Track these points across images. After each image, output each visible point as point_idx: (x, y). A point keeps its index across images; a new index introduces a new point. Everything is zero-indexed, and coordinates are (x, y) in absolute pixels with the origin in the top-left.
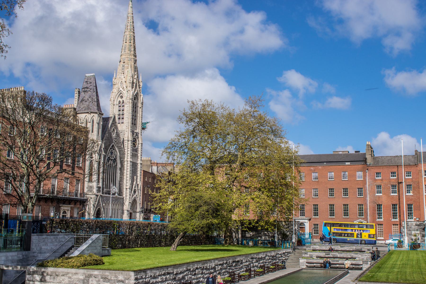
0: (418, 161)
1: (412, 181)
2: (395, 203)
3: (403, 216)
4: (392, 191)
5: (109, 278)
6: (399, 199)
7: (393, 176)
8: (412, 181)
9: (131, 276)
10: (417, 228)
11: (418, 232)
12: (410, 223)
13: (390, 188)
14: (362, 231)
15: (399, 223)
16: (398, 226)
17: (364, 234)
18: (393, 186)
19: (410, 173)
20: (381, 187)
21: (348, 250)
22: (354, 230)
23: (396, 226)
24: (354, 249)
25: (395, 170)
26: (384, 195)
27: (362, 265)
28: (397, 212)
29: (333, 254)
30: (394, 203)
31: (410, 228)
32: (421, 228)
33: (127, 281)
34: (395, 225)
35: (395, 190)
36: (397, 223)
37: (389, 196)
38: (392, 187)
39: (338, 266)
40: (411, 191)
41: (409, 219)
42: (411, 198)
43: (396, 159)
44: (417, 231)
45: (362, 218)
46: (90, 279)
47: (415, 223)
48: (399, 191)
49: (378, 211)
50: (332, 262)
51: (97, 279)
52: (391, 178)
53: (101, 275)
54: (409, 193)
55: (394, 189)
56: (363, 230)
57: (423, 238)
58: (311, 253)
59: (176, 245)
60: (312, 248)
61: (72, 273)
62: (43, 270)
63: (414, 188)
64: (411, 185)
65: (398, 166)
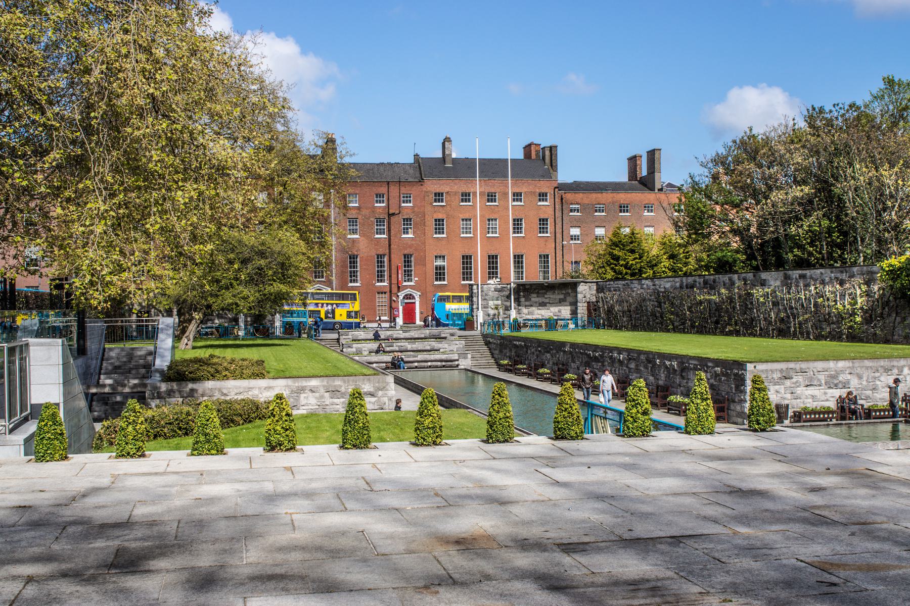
0: (423, 176)
1: (413, 212)
2: (381, 253)
3: (396, 276)
4: (377, 229)
5: (343, 389)
6: (390, 245)
8: (413, 212)
9: (388, 384)
10: (497, 296)
11: (499, 302)
12: (485, 286)
13: (373, 224)
14: (335, 306)
15: (388, 290)
16: (387, 295)
17: (338, 311)
18: (380, 221)
19: (410, 197)
20: (356, 222)
21: (416, 336)
22: (320, 305)
23: (384, 295)
24: (427, 335)
25: (383, 190)
26: (363, 238)
27: (458, 360)
28: (385, 269)
29: (399, 344)
30: (381, 252)
31: (486, 295)
32: (503, 296)
33: (380, 393)
34: (382, 293)
35: (382, 227)
38: (377, 222)
39: (416, 364)
40: (410, 230)
41: (405, 281)
42: (410, 243)
43: (382, 169)
45: (321, 281)
46: (302, 396)
47: (494, 286)
48: (389, 230)
49: (351, 268)
51: (317, 395)
52: (376, 205)
53: (324, 386)
54: (407, 233)
55: (380, 225)
56: (336, 304)
57: (506, 312)
58: (359, 346)
59: (191, 337)
60: (350, 337)
61: (260, 388)
62: (191, 385)
63: (416, 224)
64: (411, 219)
65: (388, 183)
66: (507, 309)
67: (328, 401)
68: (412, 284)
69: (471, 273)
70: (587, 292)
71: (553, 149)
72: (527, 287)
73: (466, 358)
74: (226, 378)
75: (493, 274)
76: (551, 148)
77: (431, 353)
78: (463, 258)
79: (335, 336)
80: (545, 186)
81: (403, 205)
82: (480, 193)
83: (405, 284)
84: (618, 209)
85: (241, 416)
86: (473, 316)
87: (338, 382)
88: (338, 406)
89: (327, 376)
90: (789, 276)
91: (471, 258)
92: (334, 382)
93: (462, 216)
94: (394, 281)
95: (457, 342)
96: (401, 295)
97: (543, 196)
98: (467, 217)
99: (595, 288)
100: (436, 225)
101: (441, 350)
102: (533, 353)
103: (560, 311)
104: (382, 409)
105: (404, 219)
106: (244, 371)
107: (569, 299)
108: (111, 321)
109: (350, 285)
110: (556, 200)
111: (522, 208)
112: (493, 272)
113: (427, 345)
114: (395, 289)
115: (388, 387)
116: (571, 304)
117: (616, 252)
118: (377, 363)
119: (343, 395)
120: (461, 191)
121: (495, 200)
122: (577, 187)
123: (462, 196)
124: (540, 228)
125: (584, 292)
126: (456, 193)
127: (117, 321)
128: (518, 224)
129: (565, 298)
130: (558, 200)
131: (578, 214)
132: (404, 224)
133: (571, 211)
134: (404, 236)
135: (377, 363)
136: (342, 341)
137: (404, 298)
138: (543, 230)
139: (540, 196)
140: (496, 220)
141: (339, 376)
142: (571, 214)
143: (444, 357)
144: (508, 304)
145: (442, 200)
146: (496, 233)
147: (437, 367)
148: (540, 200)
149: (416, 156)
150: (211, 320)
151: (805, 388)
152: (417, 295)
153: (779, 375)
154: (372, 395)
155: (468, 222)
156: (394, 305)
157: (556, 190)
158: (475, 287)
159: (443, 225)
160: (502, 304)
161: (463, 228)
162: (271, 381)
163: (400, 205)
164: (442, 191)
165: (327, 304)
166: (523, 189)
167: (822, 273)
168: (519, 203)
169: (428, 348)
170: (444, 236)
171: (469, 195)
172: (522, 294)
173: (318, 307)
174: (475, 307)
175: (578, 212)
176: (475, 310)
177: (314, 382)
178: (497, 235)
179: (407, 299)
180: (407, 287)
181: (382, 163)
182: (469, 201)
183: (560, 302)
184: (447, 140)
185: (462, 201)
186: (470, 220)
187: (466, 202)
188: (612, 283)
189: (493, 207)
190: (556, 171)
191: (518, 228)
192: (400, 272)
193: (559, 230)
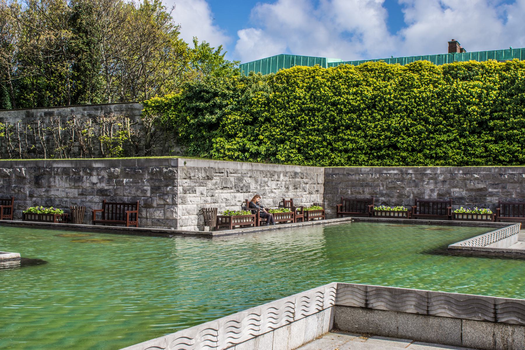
90: (32, 115)
151: (221, 191)
153: (204, 175)
167: (72, 111)
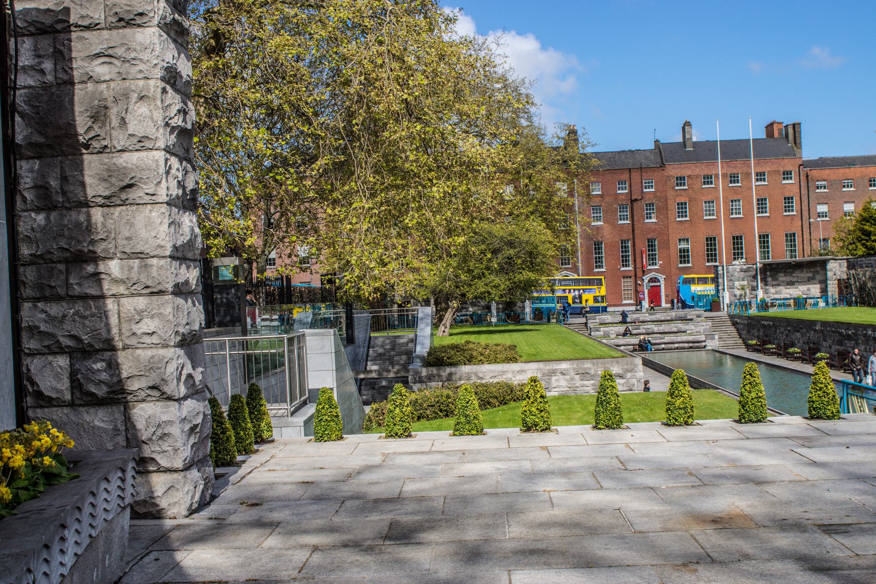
2: (625, 238)
4: (620, 216)
5: (592, 372)
6: (633, 231)
7: (622, 188)
9: (636, 365)
10: (743, 276)
11: (745, 283)
12: (731, 267)
13: (616, 211)
14: (581, 291)
15: (633, 274)
16: (632, 279)
17: (585, 296)
18: (622, 207)
21: (663, 318)
22: (567, 291)
23: (629, 280)
24: (674, 317)
25: (625, 176)
27: (705, 341)
28: (630, 254)
29: (646, 327)
30: (625, 237)
31: (732, 276)
32: (750, 276)
33: (629, 375)
34: (627, 277)
35: (625, 214)
36: (630, 275)
37: (615, 226)
38: (620, 208)
39: (663, 346)
40: (652, 215)
41: (650, 265)
43: (623, 156)
44: (743, 280)
45: (568, 268)
46: (554, 378)
47: (739, 267)
50: (653, 341)
51: (568, 377)
52: (619, 192)
53: (574, 369)
54: (650, 218)
55: (623, 211)
56: (583, 289)
57: (753, 292)
58: (606, 329)
59: (448, 325)
61: (513, 372)
62: (448, 370)
63: (658, 209)
64: (653, 204)
65: (630, 170)
66: (754, 289)
67: (578, 383)
68: (657, 267)
69: (715, 255)
70: (837, 269)
71: (796, 126)
72: (774, 266)
73: (713, 339)
74: (481, 362)
75: (738, 255)
76: (794, 125)
77: (678, 334)
78: (707, 241)
79: (583, 320)
80: (789, 164)
81: (645, 190)
82: (722, 175)
83: (649, 267)
84: (867, 183)
85: (497, 398)
86: (718, 297)
87: (587, 365)
88: (588, 388)
89: (576, 359)
91: (715, 240)
92: (583, 364)
93: (704, 199)
94: (639, 265)
95: (704, 324)
96: (646, 278)
97: (787, 174)
98: (709, 199)
99: (846, 265)
100: (678, 208)
101: (688, 332)
102: (782, 333)
103: (809, 290)
104: (631, 390)
105: (646, 204)
106: (498, 356)
107: (819, 277)
108: (376, 312)
109: (596, 270)
110: (801, 178)
111: (767, 187)
112: (738, 253)
113: (673, 327)
114: (639, 274)
115: (636, 369)
116: (820, 282)
117: (866, 227)
118: (624, 345)
119: (593, 377)
120: (703, 174)
121: (738, 180)
122: (822, 163)
123: (704, 178)
124: (785, 207)
125: (834, 270)
126: (697, 176)
127: (380, 312)
128: (762, 204)
129: (814, 276)
130: (803, 178)
131: (825, 190)
132: (647, 210)
133: (818, 188)
134: (647, 221)
135: (624, 345)
136: (590, 325)
137: (649, 281)
138: (788, 208)
139: (784, 174)
140: (739, 201)
141: (588, 359)
142: (817, 191)
143: (691, 338)
144: (755, 284)
145: (684, 183)
146: (739, 213)
147: (684, 348)
148: (784, 179)
149: (656, 142)
150: (465, 308)
152: (662, 278)
154: (621, 377)
155: (711, 204)
156: (639, 289)
157: (801, 167)
158: (720, 268)
159: (686, 208)
160: (748, 284)
161: (706, 210)
162: (523, 364)
163: (642, 190)
164: (683, 175)
165: (574, 290)
166: (766, 168)
168: (762, 183)
169: (675, 330)
170: (688, 219)
171: (711, 178)
172: (768, 273)
173: (565, 292)
174: (720, 288)
175: (825, 188)
176: (721, 291)
177: (564, 366)
178: (741, 216)
179: (652, 282)
180: (651, 271)
181: (623, 151)
182: (711, 184)
183: (809, 281)
184: (687, 124)
185: (704, 184)
186: (713, 202)
187: (708, 184)
188: (864, 259)
189: (735, 188)
190: (800, 148)
191: (762, 208)
192: (644, 256)
193: (805, 208)
